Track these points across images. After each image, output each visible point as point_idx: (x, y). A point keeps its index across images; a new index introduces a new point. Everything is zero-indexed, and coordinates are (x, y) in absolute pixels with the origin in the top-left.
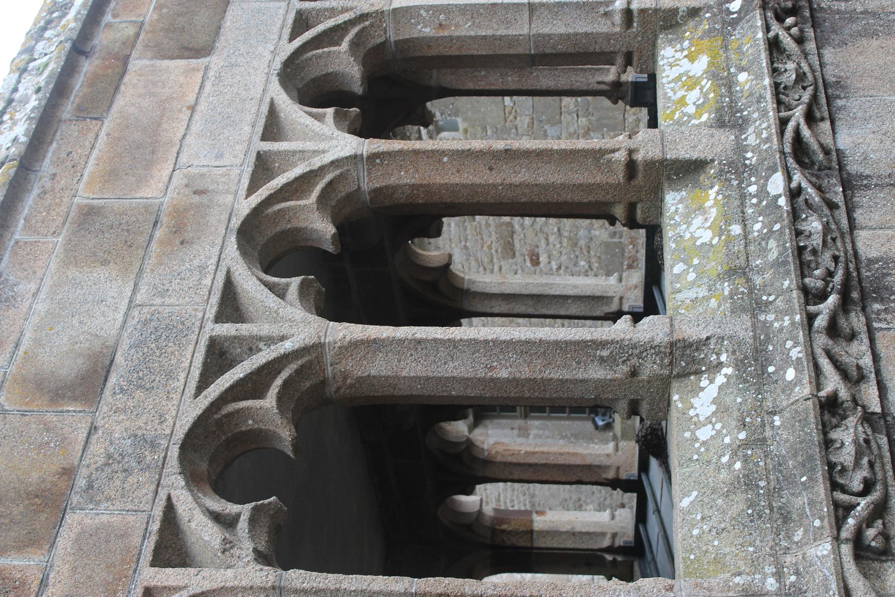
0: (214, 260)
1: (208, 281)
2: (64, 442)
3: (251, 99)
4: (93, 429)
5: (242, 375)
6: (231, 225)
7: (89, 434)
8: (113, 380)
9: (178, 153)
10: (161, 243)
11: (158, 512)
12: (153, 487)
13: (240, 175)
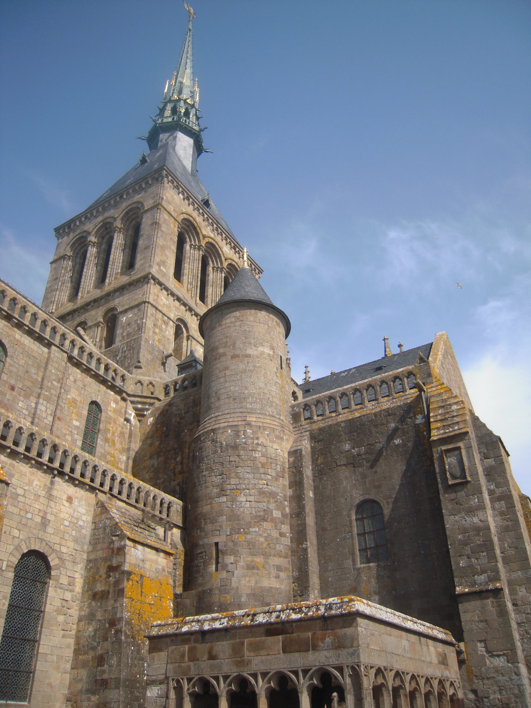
2: (202, 657)
4: (204, 661)
8: (212, 661)
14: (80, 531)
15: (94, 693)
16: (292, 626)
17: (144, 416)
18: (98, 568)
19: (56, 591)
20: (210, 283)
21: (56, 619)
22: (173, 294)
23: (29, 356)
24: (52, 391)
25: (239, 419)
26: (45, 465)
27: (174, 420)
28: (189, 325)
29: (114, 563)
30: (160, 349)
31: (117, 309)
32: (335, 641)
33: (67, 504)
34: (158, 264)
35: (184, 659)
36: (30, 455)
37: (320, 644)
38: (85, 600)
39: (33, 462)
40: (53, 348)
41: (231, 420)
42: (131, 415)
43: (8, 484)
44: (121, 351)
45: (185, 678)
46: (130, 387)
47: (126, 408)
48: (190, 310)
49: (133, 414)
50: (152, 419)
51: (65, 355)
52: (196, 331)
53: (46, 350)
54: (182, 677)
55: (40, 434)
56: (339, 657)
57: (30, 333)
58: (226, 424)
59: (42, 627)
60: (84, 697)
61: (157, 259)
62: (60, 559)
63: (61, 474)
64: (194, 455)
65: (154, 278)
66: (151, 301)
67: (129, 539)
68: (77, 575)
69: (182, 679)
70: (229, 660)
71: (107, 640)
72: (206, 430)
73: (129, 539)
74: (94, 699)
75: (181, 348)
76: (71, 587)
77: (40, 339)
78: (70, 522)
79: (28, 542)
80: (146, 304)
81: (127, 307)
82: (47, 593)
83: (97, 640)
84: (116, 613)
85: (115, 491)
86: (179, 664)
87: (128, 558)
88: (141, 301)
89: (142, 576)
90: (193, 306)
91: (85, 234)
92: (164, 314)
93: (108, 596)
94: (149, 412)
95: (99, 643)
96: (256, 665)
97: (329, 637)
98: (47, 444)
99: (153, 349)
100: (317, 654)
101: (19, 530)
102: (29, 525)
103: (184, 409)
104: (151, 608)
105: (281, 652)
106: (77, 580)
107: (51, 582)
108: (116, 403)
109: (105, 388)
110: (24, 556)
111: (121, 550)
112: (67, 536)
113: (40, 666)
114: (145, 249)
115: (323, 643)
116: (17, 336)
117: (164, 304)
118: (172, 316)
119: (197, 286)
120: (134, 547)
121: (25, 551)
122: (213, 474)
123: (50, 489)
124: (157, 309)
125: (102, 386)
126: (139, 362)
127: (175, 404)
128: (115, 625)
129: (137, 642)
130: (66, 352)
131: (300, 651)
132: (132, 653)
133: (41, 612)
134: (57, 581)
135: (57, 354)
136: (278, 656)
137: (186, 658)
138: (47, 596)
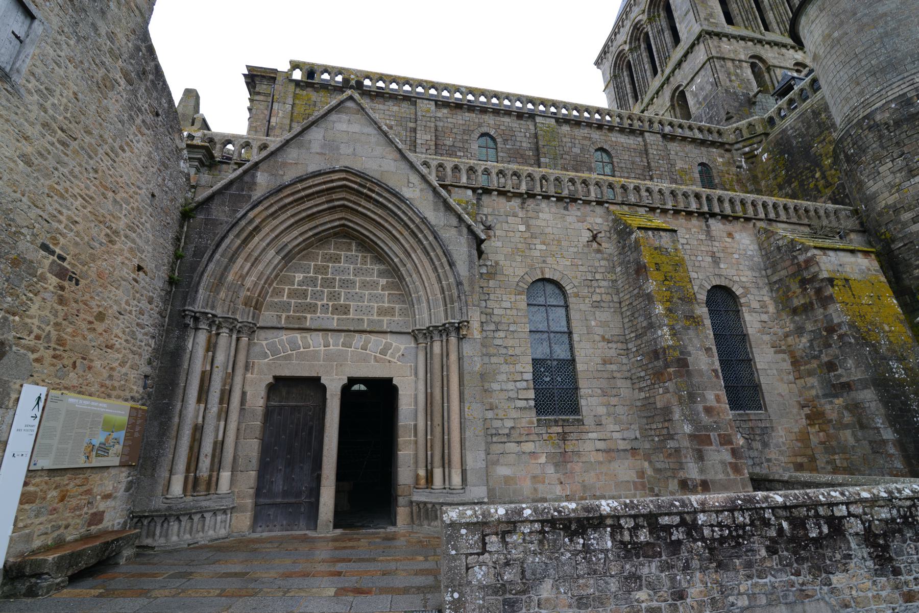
14: (752, 260)
15: (836, 396)
17: (755, 156)
18: (788, 287)
19: (751, 315)
20: (768, 8)
21: (762, 339)
22: (735, 37)
23: (629, 149)
24: (661, 169)
25: (903, 87)
26: (694, 212)
27: (795, 142)
28: (764, 57)
29: (807, 275)
30: (743, 93)
31: (681, 85)
33: (729, 240)
34: (705, 19)
36: (679, 208)
38: (784, 317)
39: (684, 213)
40: (647, 134)
41: (889, 94)
42: (741, 161)
43: (675, 231)
44: (703, 115)
46: (732, 138)
47: (733, 158)
48: (760, 41)
49: (743, 160)
50: (766, 155)
51: (659, 136)
52: (774, 58)
53: (640, 139)
55: (679, 189)
57: (622, 130)
58: (884, 101)
59: (751, 348)
60: (823, 401)
61: (702, 15)
62: (743, 288)
63: (713, 215)
64: (846, 155)
65: (710, 34)
66: (714, 54)
67: (815, 248)
68: (766, 298)
71: (830, 346)
72: (854, 122)
73: (815, 248)
74: (839, 401)
75: (765, 82)
76: (764, 310)
77: (632, 132)
78: (739, 254)
79: (708, 280)
80: (711, 61)
81: (692, 76)
82: (744, 318)
83: (818, 349)
84: (832, 320)
85: (772, 215)
87: (823, 267)
88: (705, 60)
89: (847, 280)
90: (760, 37)
91: (621, 48)
92: (733, 60)
93: (813, 309)
94: (760, 150)
95: (821, 352)
98: (689, 196)
99: (737, 96)
101: (697, 273)
102: (703, 266)
103: (804, 126)
104: (872, 308)
106: (767, 302)
107: (744, 308)
108: (723, 157)
109: (706, 149)
110: (709, 291)
111: (809, 262)
112: (741, 267)
113: (763, 380)
114: (685, 15)
116: (613, 139)
117: (729, 51)
118: (743, 57)
119: (756, 18)
120: (825, 254)
121: (709, 288)
122: (887, 161)
123: (708, 232)
124: (724, 59)
125: (702, 148)
126: (728, 113)
127: (789, 128)
128: (837, 331)
129: (871, 342)
130: (659, 133)
132: (870, 353)
133: (745, 335)
134: (749, 306)
135: (651, 138)
138: (745, 321)
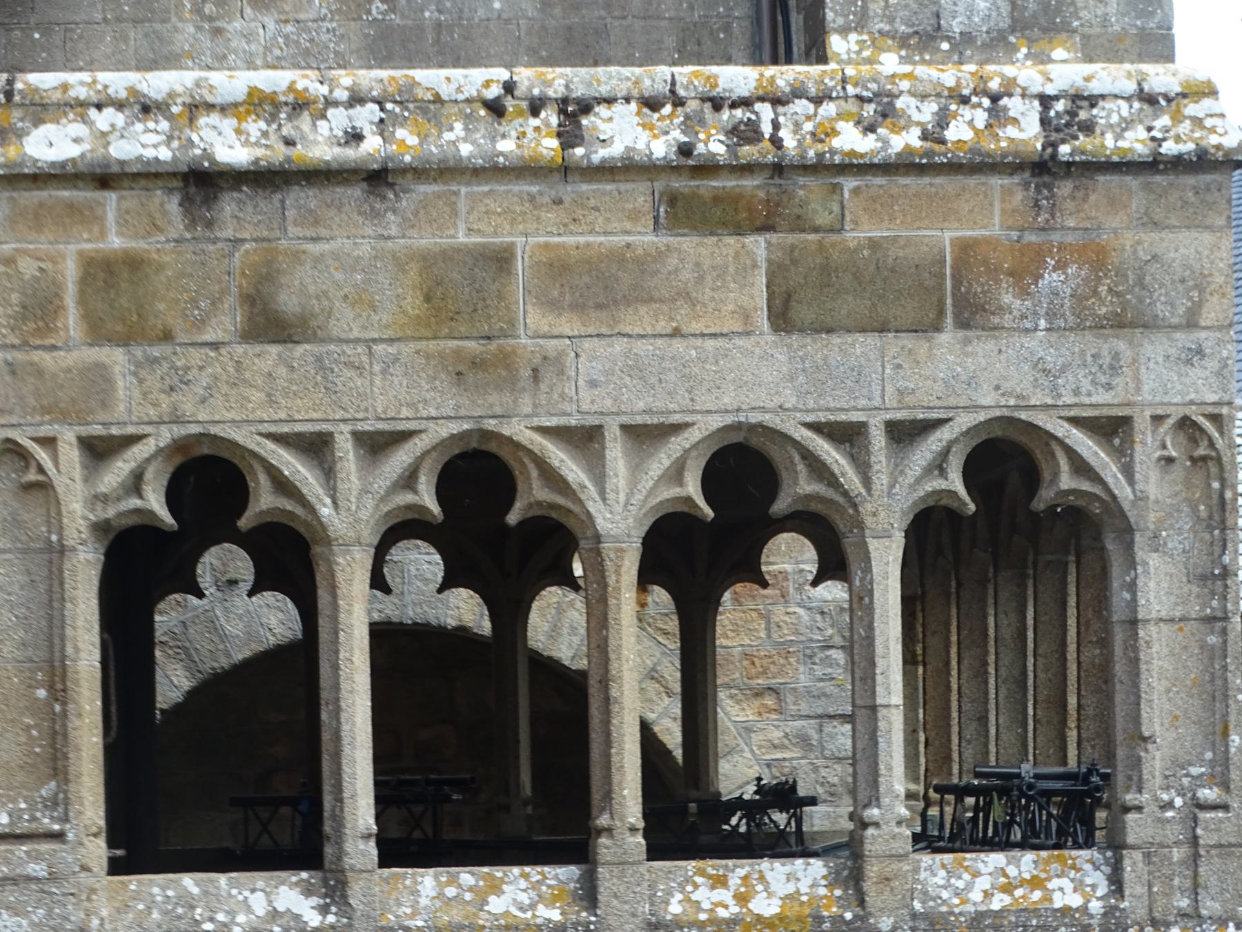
0: (433, 413)
1: (405, 412)
2: (201, 324)
3: (692, 400)
4: (215, 346)
5: (286, 473)
6: (485, 421)
7: (212, 344)
9: (598, 335)
10: (457, 352)
11: (131, 430)
12: (156, 419)
13: (565, 414)
16: (836, 188)
32: (1095, 293)
35: (47, 329)
37: (1007, 299)
45: (68, 437)
54: (45, 431)
56: (1114, 369)
69: (49, 442)
70: (408, 349)
86: (20, 356)
96: (593, 384)
97: (1060, 266)
100: (983, 348)
105: (762, 320)
115: (1024, 293)
131: (882, 329)
136: (739, 342)
137: (72, 321)
